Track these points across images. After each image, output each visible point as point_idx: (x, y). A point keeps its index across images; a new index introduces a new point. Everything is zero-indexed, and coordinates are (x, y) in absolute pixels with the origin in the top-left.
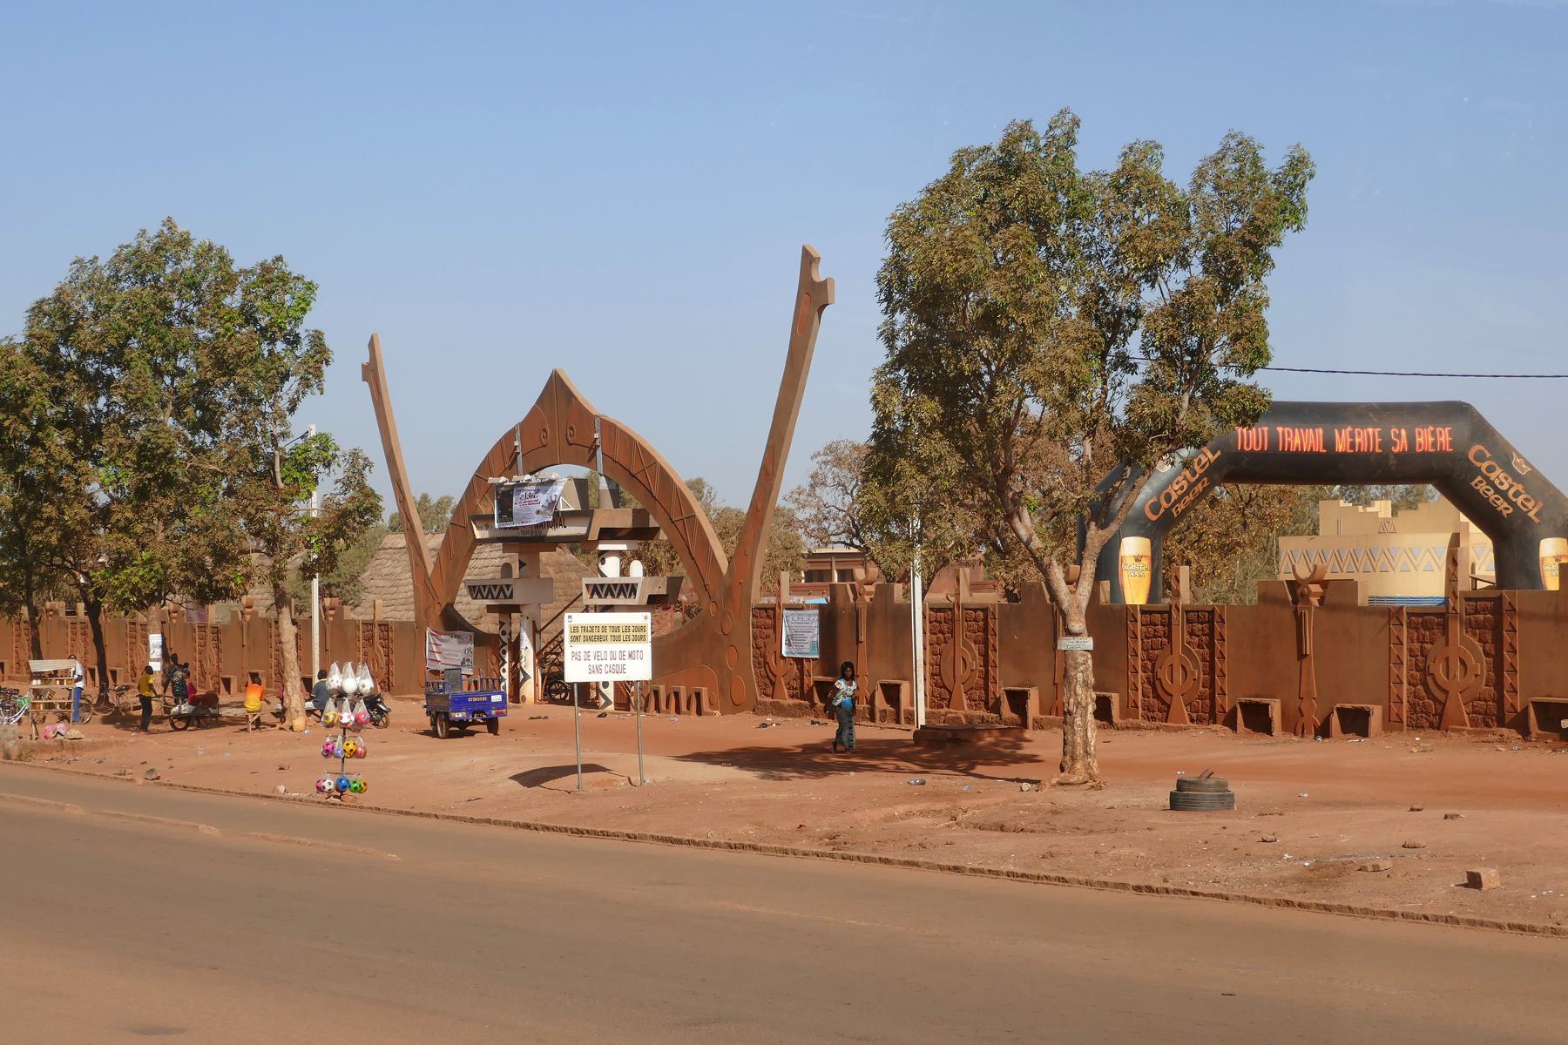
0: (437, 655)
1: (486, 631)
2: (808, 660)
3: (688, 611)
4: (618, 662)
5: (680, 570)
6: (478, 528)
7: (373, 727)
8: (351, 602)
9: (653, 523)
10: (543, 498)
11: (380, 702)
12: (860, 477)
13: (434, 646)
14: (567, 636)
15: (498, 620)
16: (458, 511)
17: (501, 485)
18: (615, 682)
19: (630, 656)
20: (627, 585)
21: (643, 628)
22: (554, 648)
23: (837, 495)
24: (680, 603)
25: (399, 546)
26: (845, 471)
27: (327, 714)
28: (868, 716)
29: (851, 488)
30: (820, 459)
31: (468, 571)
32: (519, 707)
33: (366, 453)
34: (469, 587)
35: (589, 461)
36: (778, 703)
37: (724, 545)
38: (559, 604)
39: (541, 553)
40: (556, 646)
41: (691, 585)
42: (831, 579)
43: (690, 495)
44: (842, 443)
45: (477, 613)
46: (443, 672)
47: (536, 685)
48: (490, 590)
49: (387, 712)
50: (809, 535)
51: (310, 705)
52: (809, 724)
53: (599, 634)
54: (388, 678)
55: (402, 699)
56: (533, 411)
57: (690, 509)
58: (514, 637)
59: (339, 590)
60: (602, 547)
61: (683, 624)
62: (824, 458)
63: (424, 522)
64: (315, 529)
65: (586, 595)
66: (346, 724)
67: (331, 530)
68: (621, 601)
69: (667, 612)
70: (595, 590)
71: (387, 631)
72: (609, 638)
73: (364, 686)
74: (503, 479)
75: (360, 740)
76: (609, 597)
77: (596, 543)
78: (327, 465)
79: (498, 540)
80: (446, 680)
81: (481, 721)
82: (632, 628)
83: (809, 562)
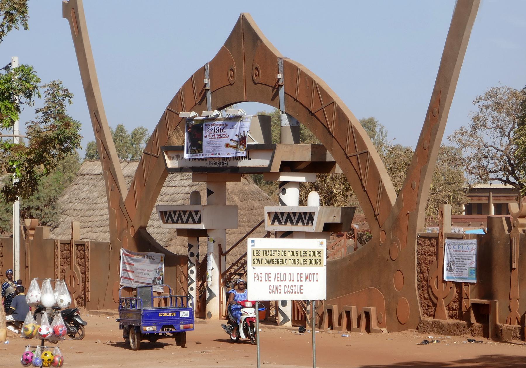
0: (130, 274)
1: (176, 253)
2: (466, 284)
3: (360, 239)
4: (296, 283)
5: (353, 201)
6: (170, 158)
7: (70, 339)
8: (49, 224)
9: (330, 158)
10: (232, 133)
11: (77, 316)
12: (517, 121)
13: (127, 266)
14: (250, 259)
15: (187, 243)
16: (151, 142)
17: (192, 119)
18: (293, 302)
19: (307, 278)
20: (305, 213)
21: (319, 253)
22: (238, 269)
23: (495, 136)
24: (353, 231)
25: (96, 172)
26: (504, 115)
27: (27, 326)
28: (519, 335)
29: (508, 130)
30: (481, 103)
31: (160, 197)
32: (205, 323)
33: (65, 85)
34: (161, 212)
35: (273, 99)
36: (439, 322)
37: (394, 179)
38: (243, 229)
39: (227, 183)
40: (240, 268)
41: (363, 215)
42: (488, 211)
43: (363, 133)
44: (501, 90)
45: (167, 237)
46: (135, 289)
47: (221, 303)
48: (180, 216)
49: (83, 325)
50: (470, 172)
51: (10, 318)
52: (466, 342)
53: (277, 257)
54: (85, 294)
55: (97, 314)
56: (222, 53)
57: (363, 145)
58: (201, 258)
59: (38, 212)
60: (283, 178)
61: (355, 250)
62: (484, 102)
63: (119, 151)
64: (17, 155)
65: (268, 221)
66: (45, 336)
67: (33, 156)
68: (300, 228)
69: (340, 239)
70: (276, 217)
71: (84, 251)
72: (288, 261)
73: (62, 301)
74: (193, 114)
75: (58, 351)
76: (289, 224)
77: (278, 174)
78: (29, 96)
79: (194, 170)
80: (139, 297)
81: (171, 335)
82: (309, 253)
83: (470, 196)
